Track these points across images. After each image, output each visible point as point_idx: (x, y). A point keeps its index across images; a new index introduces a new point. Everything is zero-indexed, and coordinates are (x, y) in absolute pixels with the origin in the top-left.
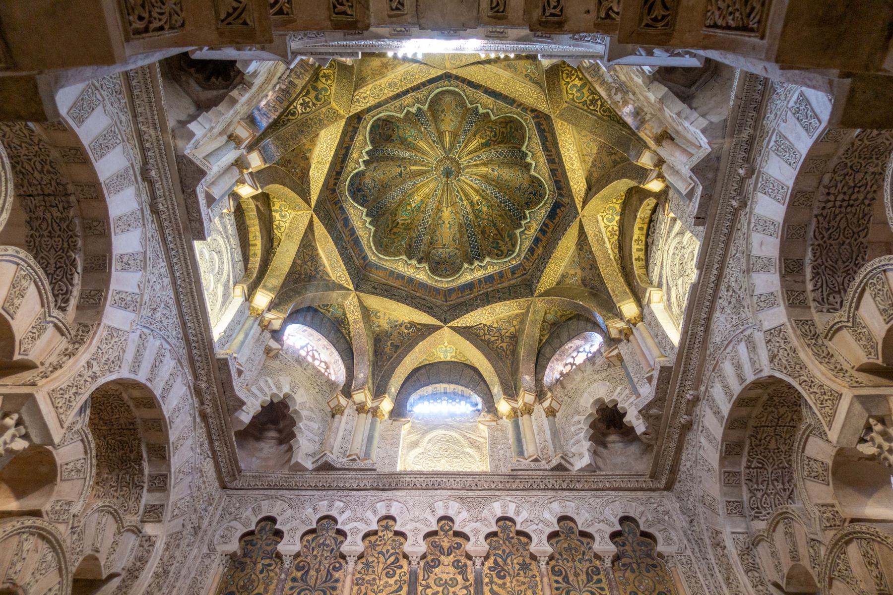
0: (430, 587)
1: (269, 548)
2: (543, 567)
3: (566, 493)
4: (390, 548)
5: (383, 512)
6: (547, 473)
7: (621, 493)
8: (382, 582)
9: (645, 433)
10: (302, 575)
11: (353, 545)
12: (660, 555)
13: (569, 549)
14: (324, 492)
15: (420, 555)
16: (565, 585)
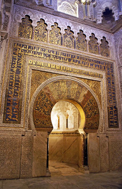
0: (65, 41)
1: (29, 24)
2: (88, 43)
3: (94, 28)
4: (56, 30)
5: (55, 22)
6: (92, 22)
7: (104, 31)
8: (55, 38)
9: (117, 21)
10: (38, 32)
11: (49, 28)
12: (108, 46)
13: (92, 40)
14: (41, 12)
15: (64, 34)
16: (90, 47)
